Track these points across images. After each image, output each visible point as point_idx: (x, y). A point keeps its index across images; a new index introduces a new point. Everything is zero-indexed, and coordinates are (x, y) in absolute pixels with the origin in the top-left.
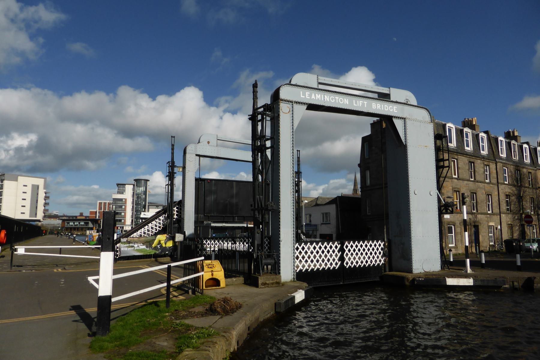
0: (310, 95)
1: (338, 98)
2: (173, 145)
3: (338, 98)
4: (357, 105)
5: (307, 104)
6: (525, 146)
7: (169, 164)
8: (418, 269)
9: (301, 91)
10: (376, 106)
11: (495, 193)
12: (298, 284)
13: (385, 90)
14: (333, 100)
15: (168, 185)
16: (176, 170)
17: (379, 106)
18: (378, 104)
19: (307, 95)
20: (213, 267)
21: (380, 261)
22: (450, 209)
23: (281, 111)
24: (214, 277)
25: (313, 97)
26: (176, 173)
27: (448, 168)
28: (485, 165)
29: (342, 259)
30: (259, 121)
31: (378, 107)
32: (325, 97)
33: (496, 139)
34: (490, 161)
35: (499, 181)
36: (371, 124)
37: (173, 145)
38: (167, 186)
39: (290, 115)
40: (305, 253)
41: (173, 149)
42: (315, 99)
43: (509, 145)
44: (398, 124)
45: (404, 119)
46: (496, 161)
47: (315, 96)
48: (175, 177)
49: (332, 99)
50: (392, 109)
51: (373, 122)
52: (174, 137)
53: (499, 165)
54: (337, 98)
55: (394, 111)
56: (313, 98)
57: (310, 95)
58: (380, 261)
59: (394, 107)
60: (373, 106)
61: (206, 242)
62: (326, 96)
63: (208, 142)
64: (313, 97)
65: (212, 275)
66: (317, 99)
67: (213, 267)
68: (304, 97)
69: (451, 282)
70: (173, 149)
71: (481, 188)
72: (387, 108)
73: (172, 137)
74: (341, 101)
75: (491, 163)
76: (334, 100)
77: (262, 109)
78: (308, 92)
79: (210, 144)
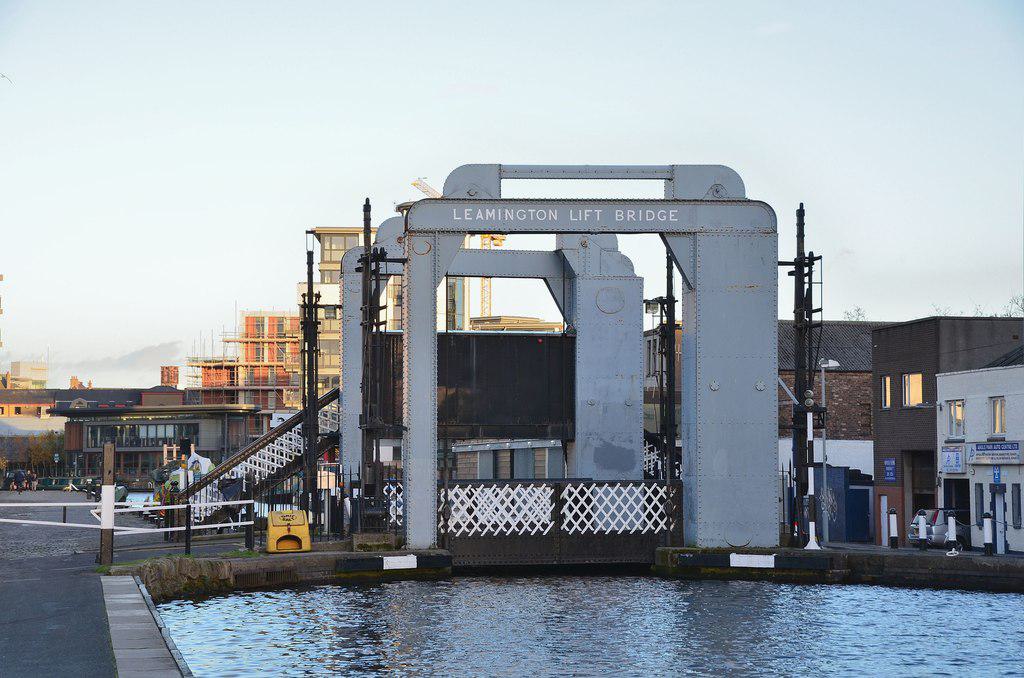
0: (473, 215)
17: (631, 213)
19: (466, 214)
24: (291, 533)
25: (480, 216)
39: (428, 258)
40: (592, 517)
57: (473, 215)
62: (507, 211)
65: (289, 530)
74: (541, 215)
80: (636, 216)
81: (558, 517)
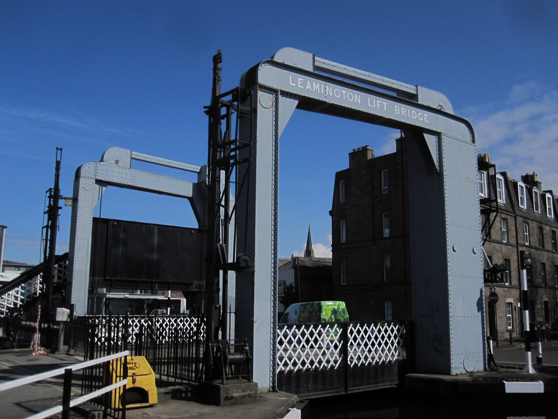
1: (346, 92)
2: (58, 163)
3: (346, 92)
4: (373, 106)
5: (299, 96)
6: (548, 195)
7: (50, 194)
8: (458, 368)
9: (291, 75)
10: (400, 110)
11: (514, 257)
12: (282, 397)
13: (409, 88)
14: (338, 96)
15: (47, 227)
16: (61, 203)
17: (404, 110)
18: (402, 108)
19: (299, 83)
20: (135, 368)
21: (393, 355)
22: (499, 275)
23: (259, 104)
24: (137, 385)
25: (308, 87)
26: (61, 208)
27: (495, 213)
28: (503, 218)
29: (344, 352)
30: (223, 117)
31: (402, 112)
32: (326, 89)
33: (515, 184)
34: (509, 213)
35: (519, 241)
36: (349, 154)
37: (58, 163)
38: (45, 230)
39: (271, 112)
41: (58, 169)
42: (311, 89)
43: (530, 191)
44: (430, 140)
45: (438, 134)
46: (516, 214)
47: (312, 88)
48: (59, 215)
49: (337, 92)
50: (422, 118)
51: (352, 151)
52: (61, 150)
53: (519, 219)
54: (344, 92)
55: (425, 121)
56: (309, 89)
57: (304, 84)
58: (393, 355)
59: (425, 115)
60: (396, 110)
61: (133, 322)
62: (327, 87)
63: (117, 162)
64: (308, 87)
66: (314, 90)
67: (135, 368)
68: (295, 85)
69: (511, 387)
70: (58, 169)
71: (497, 250)
72: (414, 116)
73: (57, 149)
75: (509, 217)
76: (339, 94)
77: (229, 97)
78: (301, 78)
79: (119, 164)
80: (407, 113)
81: (344, 352)
